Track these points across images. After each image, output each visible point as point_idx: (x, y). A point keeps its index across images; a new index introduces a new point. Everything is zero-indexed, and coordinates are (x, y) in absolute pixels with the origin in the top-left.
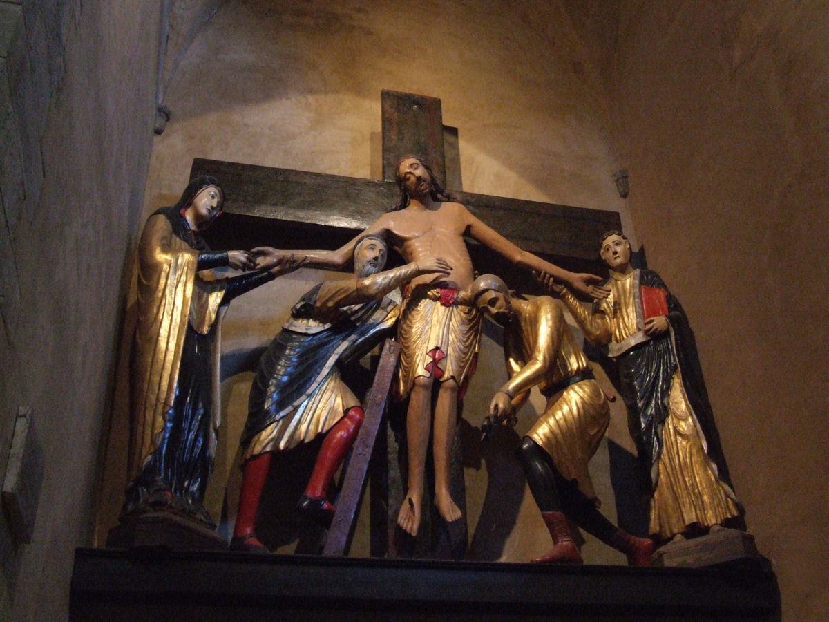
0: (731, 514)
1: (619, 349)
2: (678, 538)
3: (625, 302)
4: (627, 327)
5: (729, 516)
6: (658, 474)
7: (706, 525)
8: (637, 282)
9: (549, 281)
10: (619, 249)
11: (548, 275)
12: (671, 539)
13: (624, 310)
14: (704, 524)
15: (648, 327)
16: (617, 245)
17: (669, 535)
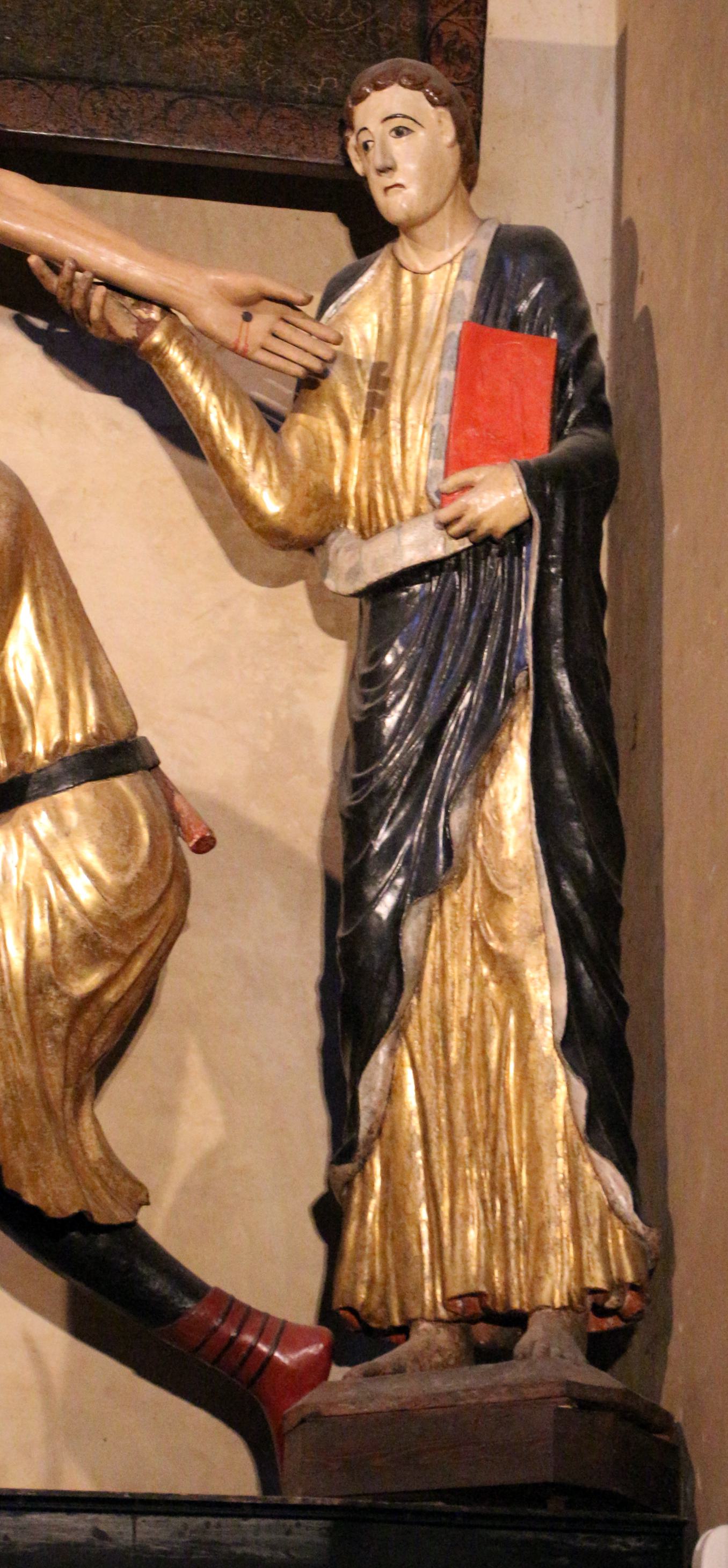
0: (607, 1270)
1: (355, 572)
2: (424, 1332)
3: (406, 385)
4: (394, 488)
5: (597, 1279)
6: (392, 1091)
7: (516, 1305)
8: (470, 289)
9: (86, 297)
10: (398, 147)
11: (88, 275)
12: (405, 1330)
13: (395, 408)
14: (507, 1302)
15: (446, 513)
16: (399, 132)
17: (397, 1321)
